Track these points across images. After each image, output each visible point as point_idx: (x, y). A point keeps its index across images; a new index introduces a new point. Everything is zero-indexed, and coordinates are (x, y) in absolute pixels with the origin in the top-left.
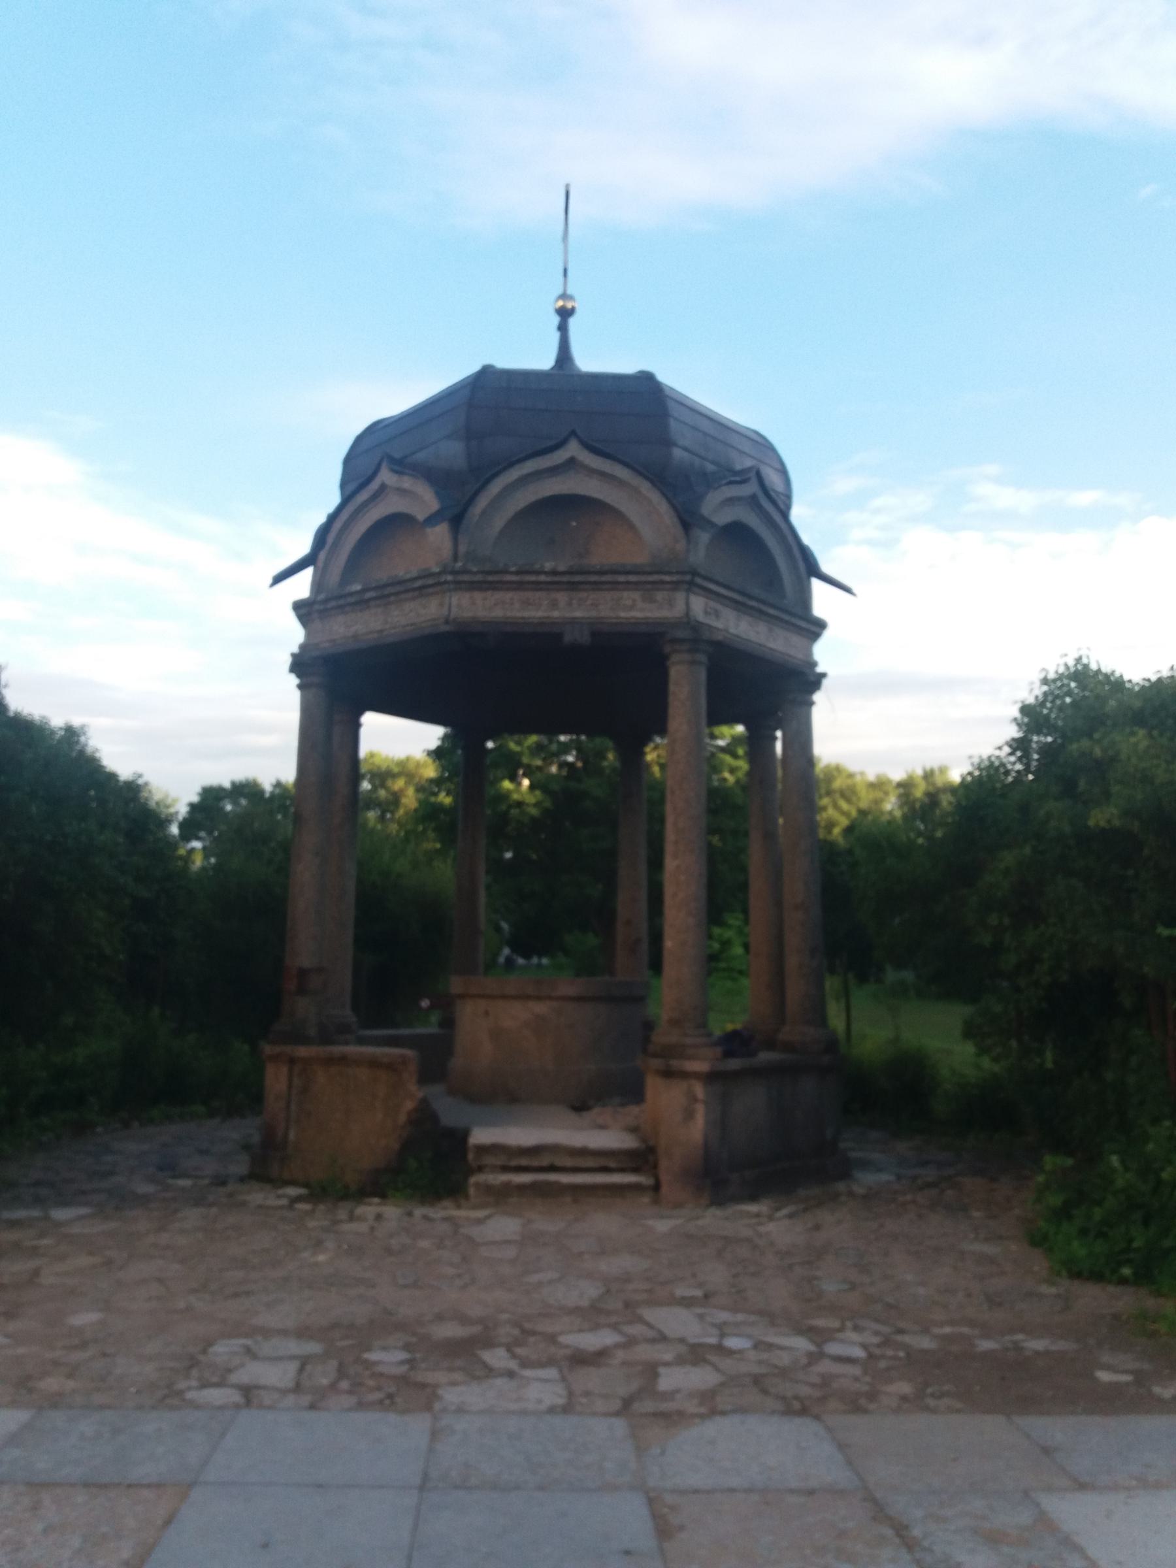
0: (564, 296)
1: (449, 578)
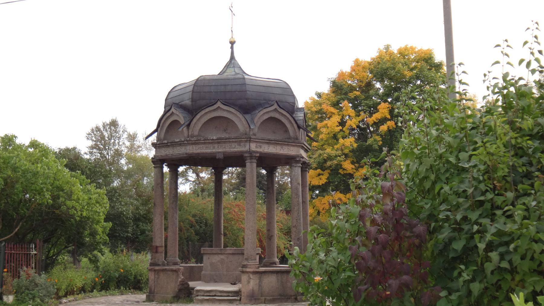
1: (186, 142)
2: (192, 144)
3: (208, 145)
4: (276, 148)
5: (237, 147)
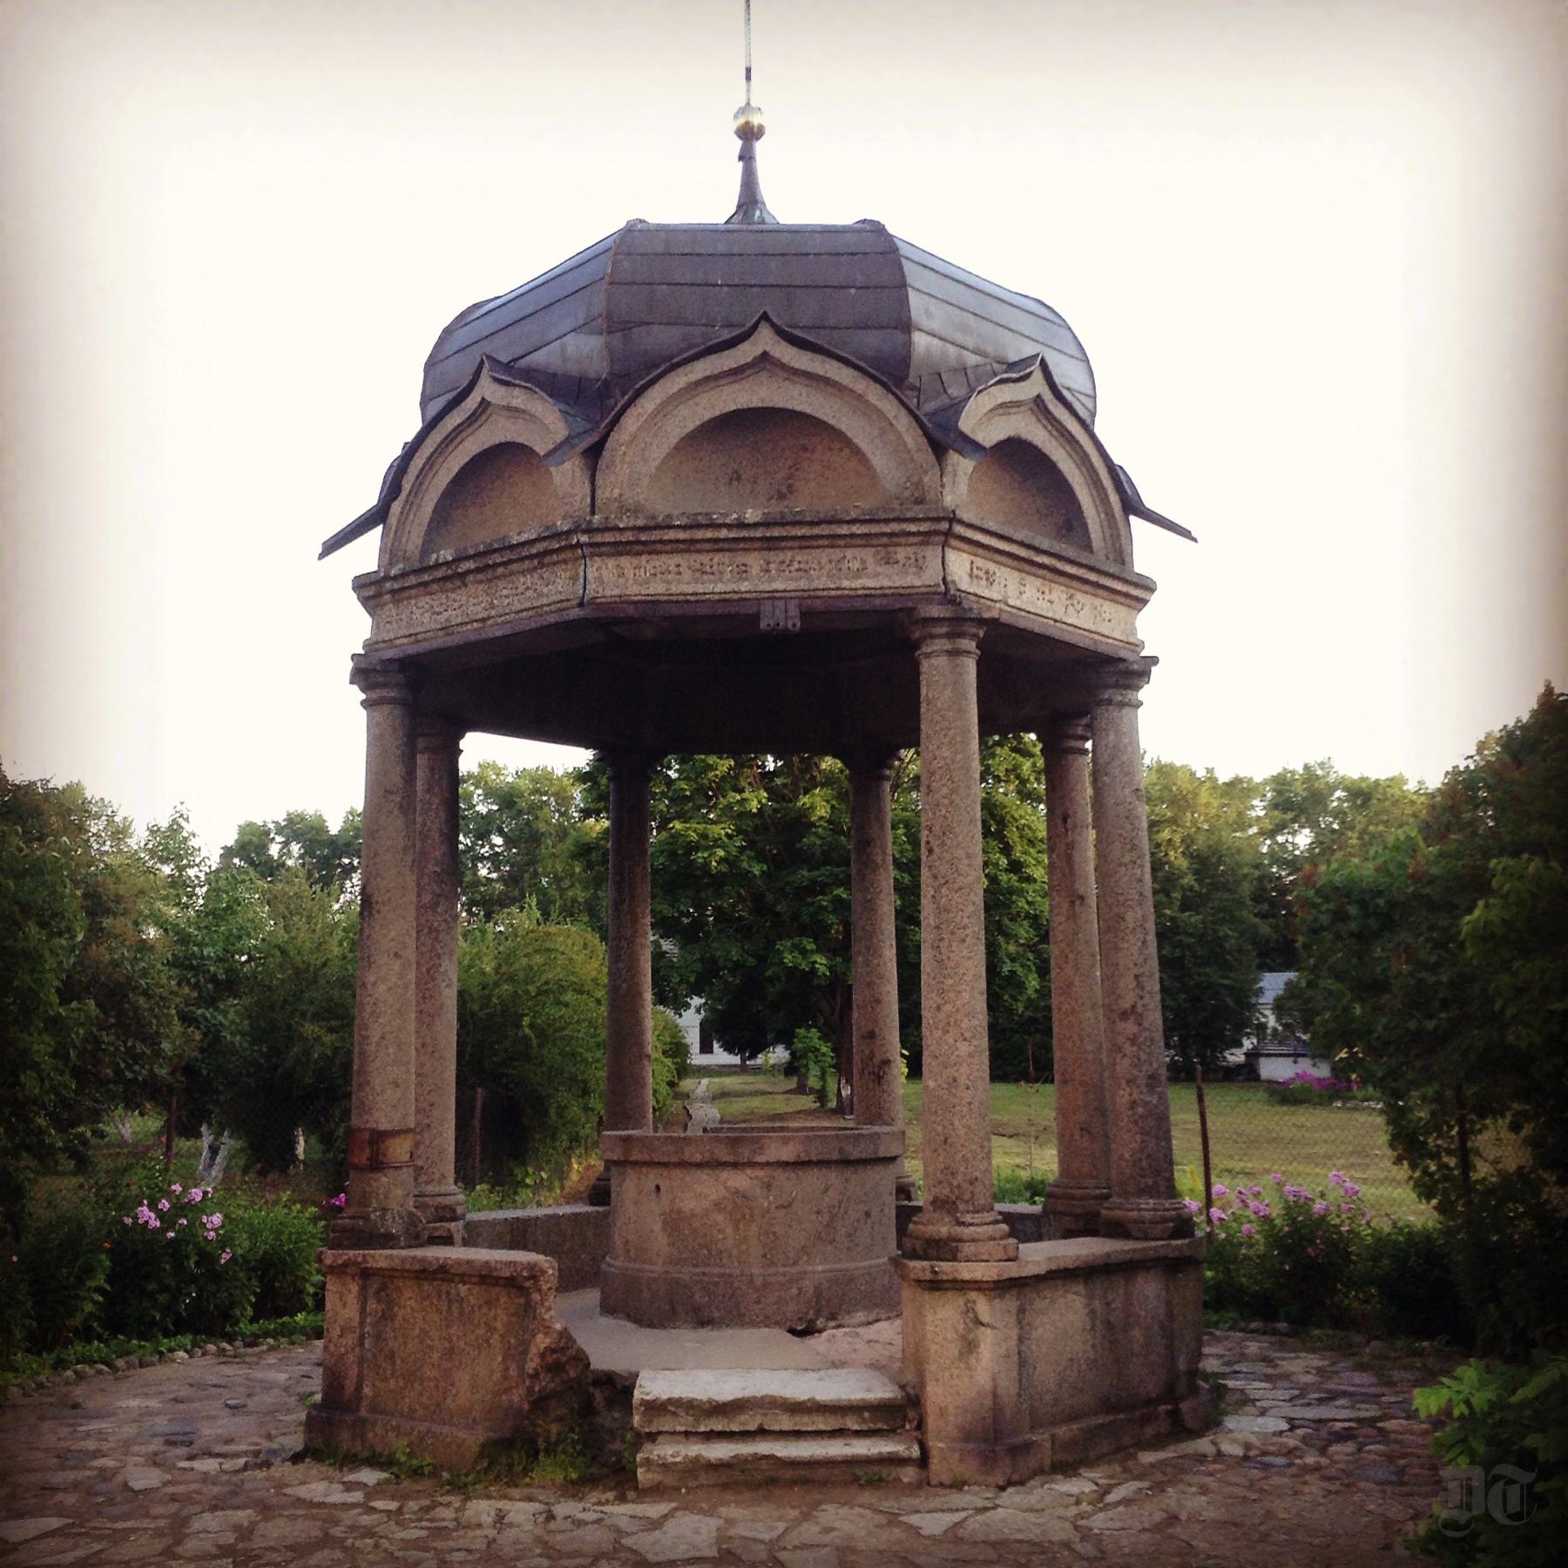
0: (747, 108)
1: (584, 539)
2: (619, 549)
3: (705, 558)
4: (1047, 597)
5: (871, 567)
